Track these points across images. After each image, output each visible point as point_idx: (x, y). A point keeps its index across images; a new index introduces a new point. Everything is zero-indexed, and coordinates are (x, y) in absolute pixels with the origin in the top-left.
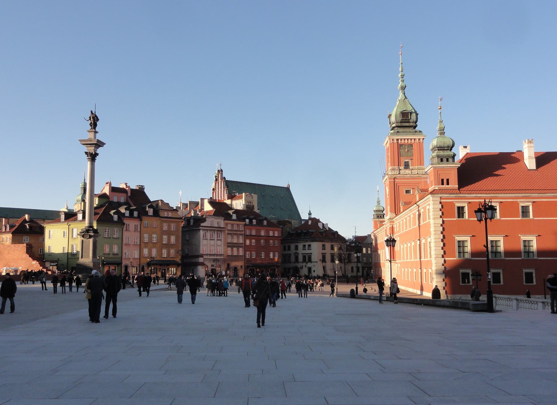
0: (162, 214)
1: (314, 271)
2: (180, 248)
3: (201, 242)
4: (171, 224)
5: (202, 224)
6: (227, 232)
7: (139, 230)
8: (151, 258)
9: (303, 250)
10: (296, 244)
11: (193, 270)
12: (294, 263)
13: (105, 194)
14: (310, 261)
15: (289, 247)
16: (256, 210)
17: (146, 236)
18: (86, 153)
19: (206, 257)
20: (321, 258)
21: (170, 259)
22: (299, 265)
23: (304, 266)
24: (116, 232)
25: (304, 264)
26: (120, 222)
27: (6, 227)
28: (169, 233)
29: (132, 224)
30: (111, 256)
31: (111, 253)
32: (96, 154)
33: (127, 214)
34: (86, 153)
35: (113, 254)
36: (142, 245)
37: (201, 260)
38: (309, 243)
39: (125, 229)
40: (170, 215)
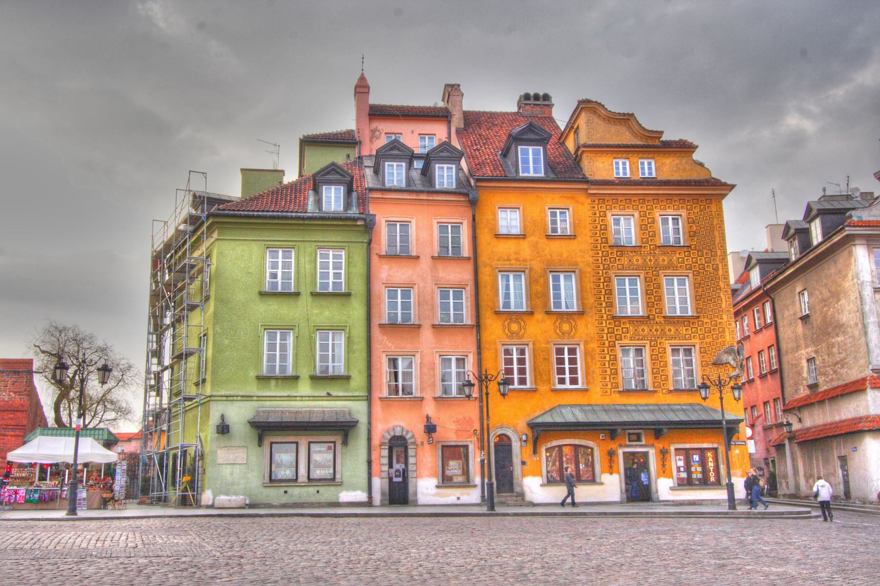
4: (657, 214)
7: (466, 251)
11: (843, 460)
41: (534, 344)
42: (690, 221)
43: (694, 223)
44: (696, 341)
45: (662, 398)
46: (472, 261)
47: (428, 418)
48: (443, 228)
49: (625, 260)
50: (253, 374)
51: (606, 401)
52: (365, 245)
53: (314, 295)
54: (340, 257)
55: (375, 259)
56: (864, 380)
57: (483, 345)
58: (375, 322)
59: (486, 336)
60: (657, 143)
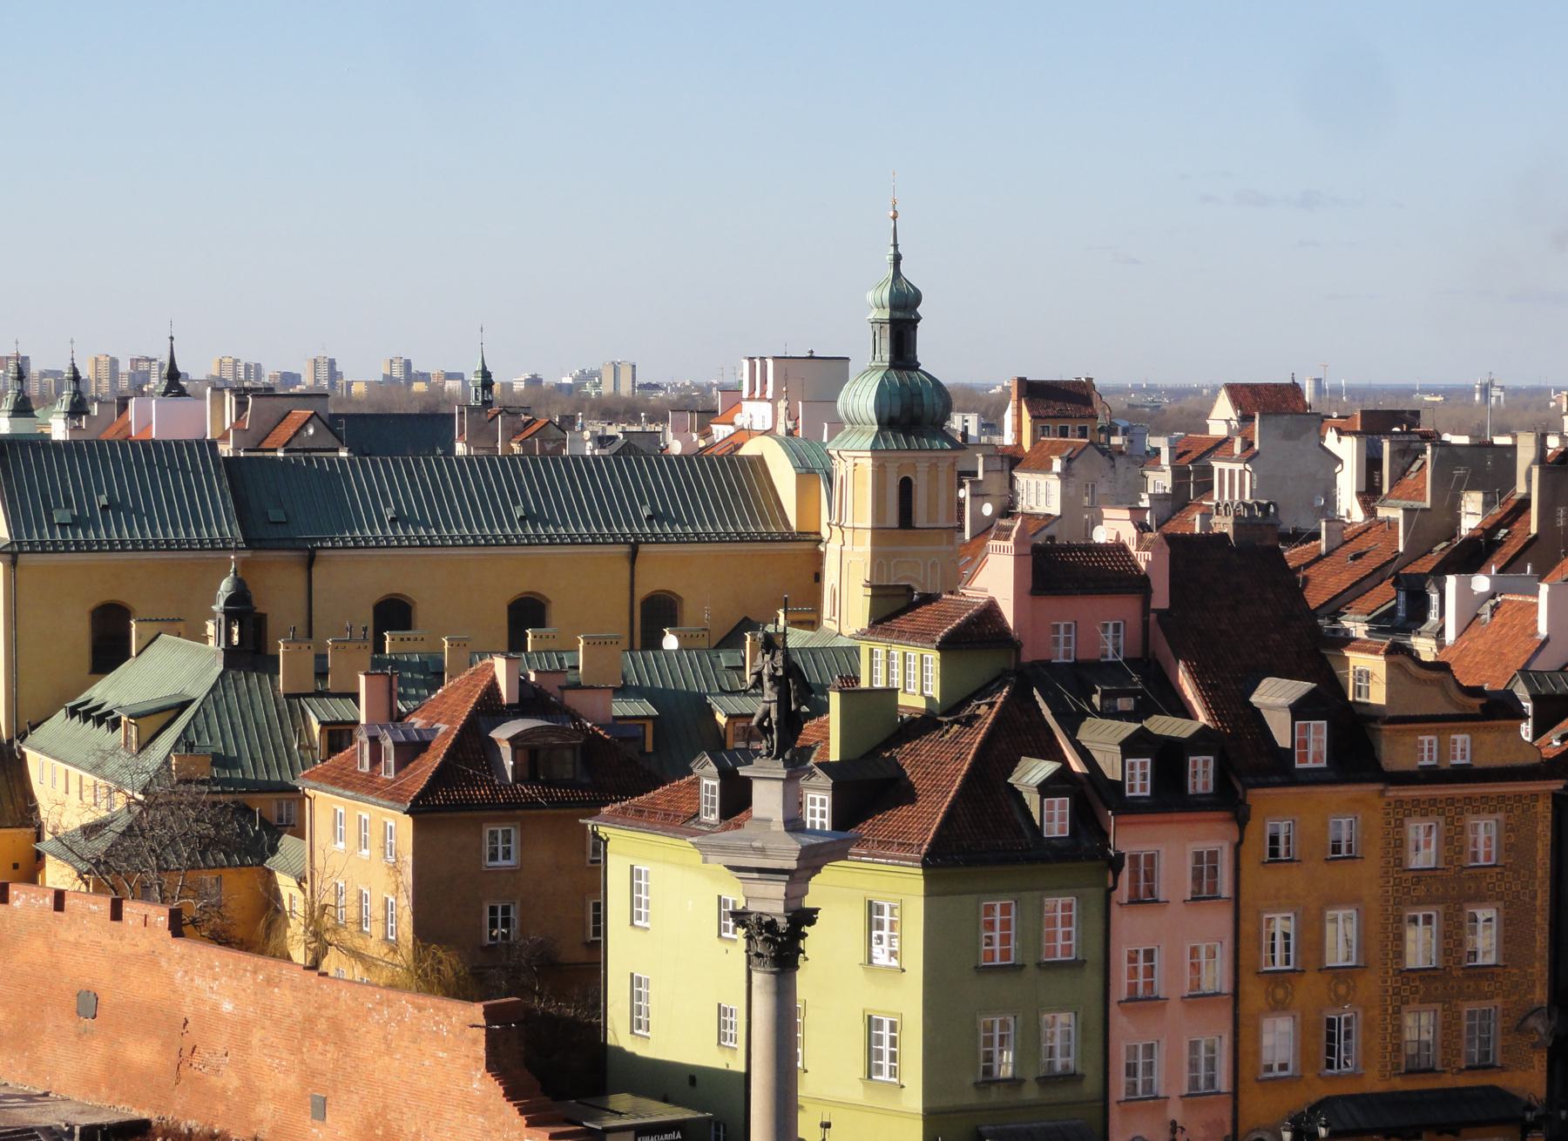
0: (1398, 751)
2: (1540, 995)
4: (1471, 820)
7: (1225, 889)
13: (990, 611)
17: (1281, 924)
18: (740, 918)
21: (1462, 1081)
24: (1061, 919)
26: (1087, 854)
27: (375, 741)
28: (1452, 889)
29: (1171, 849)
30: (1031, 1093)
31: (1030, 1075)
32: (803, 918)
33: (1139, 778)
34: (740, 918)
35: (1050, 1080)
36: (1254, 994)
39: (1123, 891)
40: (1462, 747)
41: (1303, 1015)
42: (1508, 828)
43: (1512, 830)
44: (1498, 1001)
45: (1448, 1081)
46: (1232, 903)
47: (1174, 1123)
48: (1198, 856)
49: (1421, 890)
50: (970, 1080)
51: (1380, 1087)
52: (1101, 892)
53: (1041, 966)
54: (1070, 906)
55: (1115, 910)
57: (1242, 1019)
58: (1114, 998)
59: (1243, 1010)
60: (1478, 711)
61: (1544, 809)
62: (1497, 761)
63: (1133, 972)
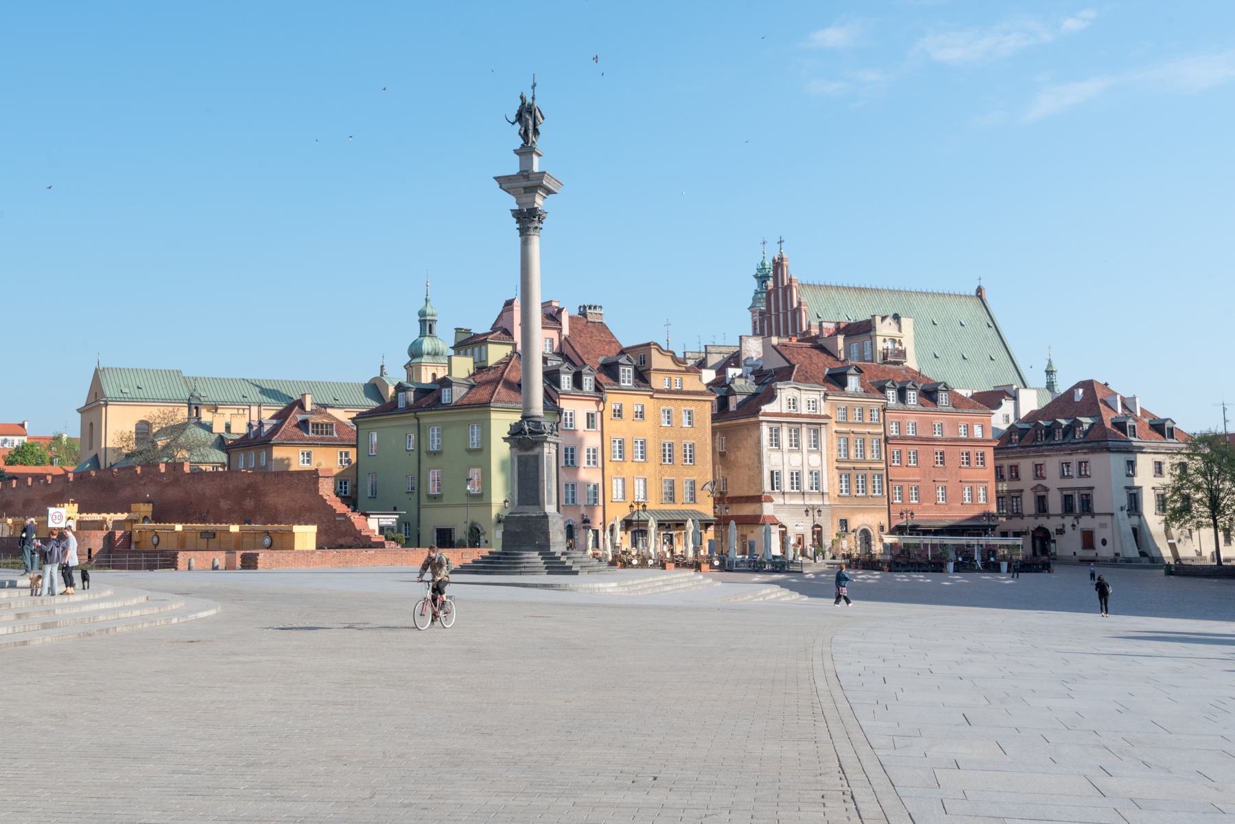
0: (658, 381)
1: (1104, 542)
3: (765, 459)
5: (766, 408)
6: (836, 428)
8: (638, 503)
9: (1063, 476)
10: (1039, 461)
12: (1036, 516)
14: (1087, 508)
15: (1015, 470)
16: (911, 362)
19: (779, 500)
20: (1124, 501)
22: (1051, 524)
23: (1068, 528)
25: (1069, 520)
37: (768, 509)
38: (1082, 457)
51: (656, 508)
56: (760, 497)
61: (708, 405)
62: (691, 389)
63: (566, 456)
